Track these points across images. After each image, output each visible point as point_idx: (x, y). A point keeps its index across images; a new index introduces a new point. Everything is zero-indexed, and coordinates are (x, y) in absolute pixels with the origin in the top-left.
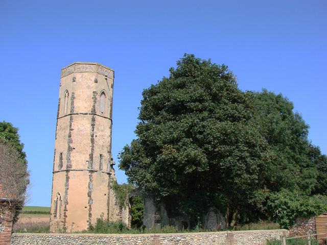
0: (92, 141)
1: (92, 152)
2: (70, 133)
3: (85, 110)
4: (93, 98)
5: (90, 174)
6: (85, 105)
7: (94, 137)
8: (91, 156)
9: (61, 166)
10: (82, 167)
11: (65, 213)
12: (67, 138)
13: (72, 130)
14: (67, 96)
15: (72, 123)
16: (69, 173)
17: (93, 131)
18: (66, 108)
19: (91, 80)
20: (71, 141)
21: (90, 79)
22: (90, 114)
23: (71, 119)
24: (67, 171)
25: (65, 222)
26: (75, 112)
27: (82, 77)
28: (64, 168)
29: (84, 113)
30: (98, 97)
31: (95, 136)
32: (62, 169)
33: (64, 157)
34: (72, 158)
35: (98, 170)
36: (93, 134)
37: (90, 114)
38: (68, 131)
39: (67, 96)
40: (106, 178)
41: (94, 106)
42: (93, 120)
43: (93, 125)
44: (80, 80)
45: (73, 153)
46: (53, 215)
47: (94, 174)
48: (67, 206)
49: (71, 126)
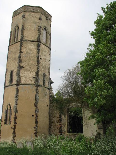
0: (38, 62)
1: (38, 70)
2: (20, 55)
3: (32, 38)
4: (38, 30)
5: (36, 88)
6: (32, 35)
7: (40, 59)
8: (37, 74)
9: (11, 81)
10: (30, 82)
11: (15, 120)
12: (17, 59)
13: (22, 52)
14: (17, 29)
15: (22, 48)
16: (19, 87)
17: (39, 54)
18: (16, 38)
19: (37, 18)
20: (20, 61)
21: (36, 17)
22: (36, 41)
23: (21, 45)
24: (17, 85)
25: (15, 128)
26: (24, 40)
27: (30, 15)
28: (15, 82)
29: (31, 40)
30: (41, 30)
31: (40, 58)
32: (13, 84)
33: (15, 74)
34: (21, 75)
35: (43, 85)
36: (39, 57)
37: (36, 41)
38: (18, 55)
39: (17, 29)
40: (48, 93)
41: (39, 36)
42: (39, 46)
43: (38, 50)
44: (28, 17)
45: (22, 71)
46: (4, 122)
47: (40, 89)
48: (17, 115)
49: (21, 49)
